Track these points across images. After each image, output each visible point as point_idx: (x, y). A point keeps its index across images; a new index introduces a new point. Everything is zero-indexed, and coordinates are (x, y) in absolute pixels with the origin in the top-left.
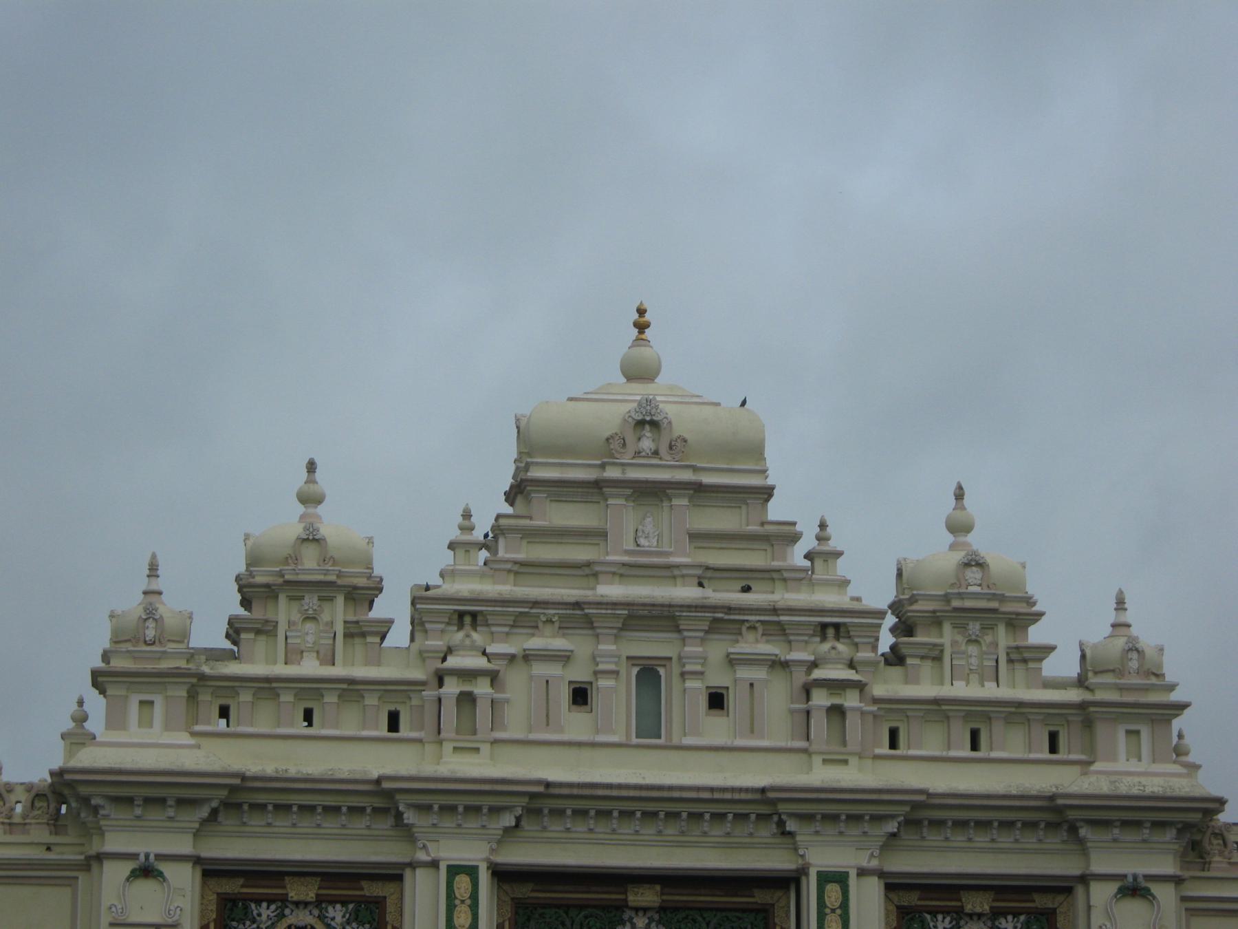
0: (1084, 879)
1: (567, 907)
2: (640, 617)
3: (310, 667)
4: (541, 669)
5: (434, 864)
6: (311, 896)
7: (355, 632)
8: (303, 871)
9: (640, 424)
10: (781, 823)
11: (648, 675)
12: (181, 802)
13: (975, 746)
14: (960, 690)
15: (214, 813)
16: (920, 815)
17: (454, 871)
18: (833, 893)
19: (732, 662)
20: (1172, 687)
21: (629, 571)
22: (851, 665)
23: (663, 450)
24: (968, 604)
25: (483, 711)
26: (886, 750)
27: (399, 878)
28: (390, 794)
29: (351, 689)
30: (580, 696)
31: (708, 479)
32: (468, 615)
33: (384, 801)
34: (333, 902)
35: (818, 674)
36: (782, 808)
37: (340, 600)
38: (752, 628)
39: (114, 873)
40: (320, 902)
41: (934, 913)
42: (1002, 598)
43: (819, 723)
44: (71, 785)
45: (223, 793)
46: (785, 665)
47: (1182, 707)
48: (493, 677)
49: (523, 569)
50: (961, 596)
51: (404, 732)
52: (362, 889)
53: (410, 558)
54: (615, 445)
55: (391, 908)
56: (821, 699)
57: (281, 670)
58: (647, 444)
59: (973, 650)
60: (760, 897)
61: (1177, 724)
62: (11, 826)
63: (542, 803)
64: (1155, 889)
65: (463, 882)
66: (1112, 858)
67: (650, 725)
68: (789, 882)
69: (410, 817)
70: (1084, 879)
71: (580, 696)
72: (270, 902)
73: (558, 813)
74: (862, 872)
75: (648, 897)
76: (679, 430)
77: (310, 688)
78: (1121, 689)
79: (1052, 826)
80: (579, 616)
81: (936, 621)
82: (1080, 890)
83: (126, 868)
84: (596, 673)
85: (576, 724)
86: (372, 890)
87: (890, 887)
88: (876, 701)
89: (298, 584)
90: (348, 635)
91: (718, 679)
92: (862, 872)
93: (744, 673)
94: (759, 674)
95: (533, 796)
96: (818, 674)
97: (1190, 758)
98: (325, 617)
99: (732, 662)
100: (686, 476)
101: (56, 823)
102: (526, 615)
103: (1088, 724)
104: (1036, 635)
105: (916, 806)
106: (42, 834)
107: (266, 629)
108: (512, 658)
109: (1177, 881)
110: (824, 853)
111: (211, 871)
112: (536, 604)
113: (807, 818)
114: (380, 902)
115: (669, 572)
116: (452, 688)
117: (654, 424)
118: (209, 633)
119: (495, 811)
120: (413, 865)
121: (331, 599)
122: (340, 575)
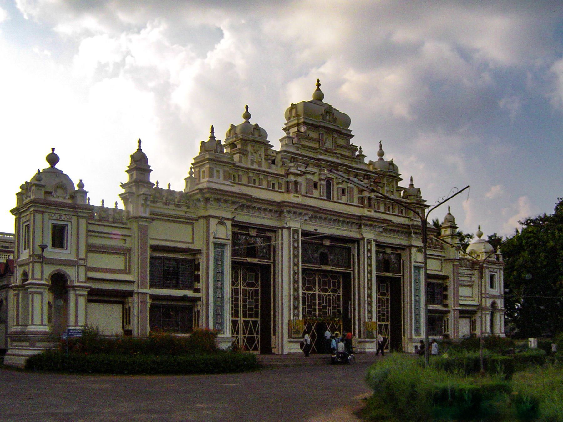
0: (410, 247)
3: (255, 167)
5: (289, 228)
11: (329, 182)
33: (279, 209)
52: (266, 233)
68: (356, 241)
72: (243, 235)
77: (258, 172)
85: (316, 193)
86: (269, 234)
98: (259, 152)
120: (282, 228)
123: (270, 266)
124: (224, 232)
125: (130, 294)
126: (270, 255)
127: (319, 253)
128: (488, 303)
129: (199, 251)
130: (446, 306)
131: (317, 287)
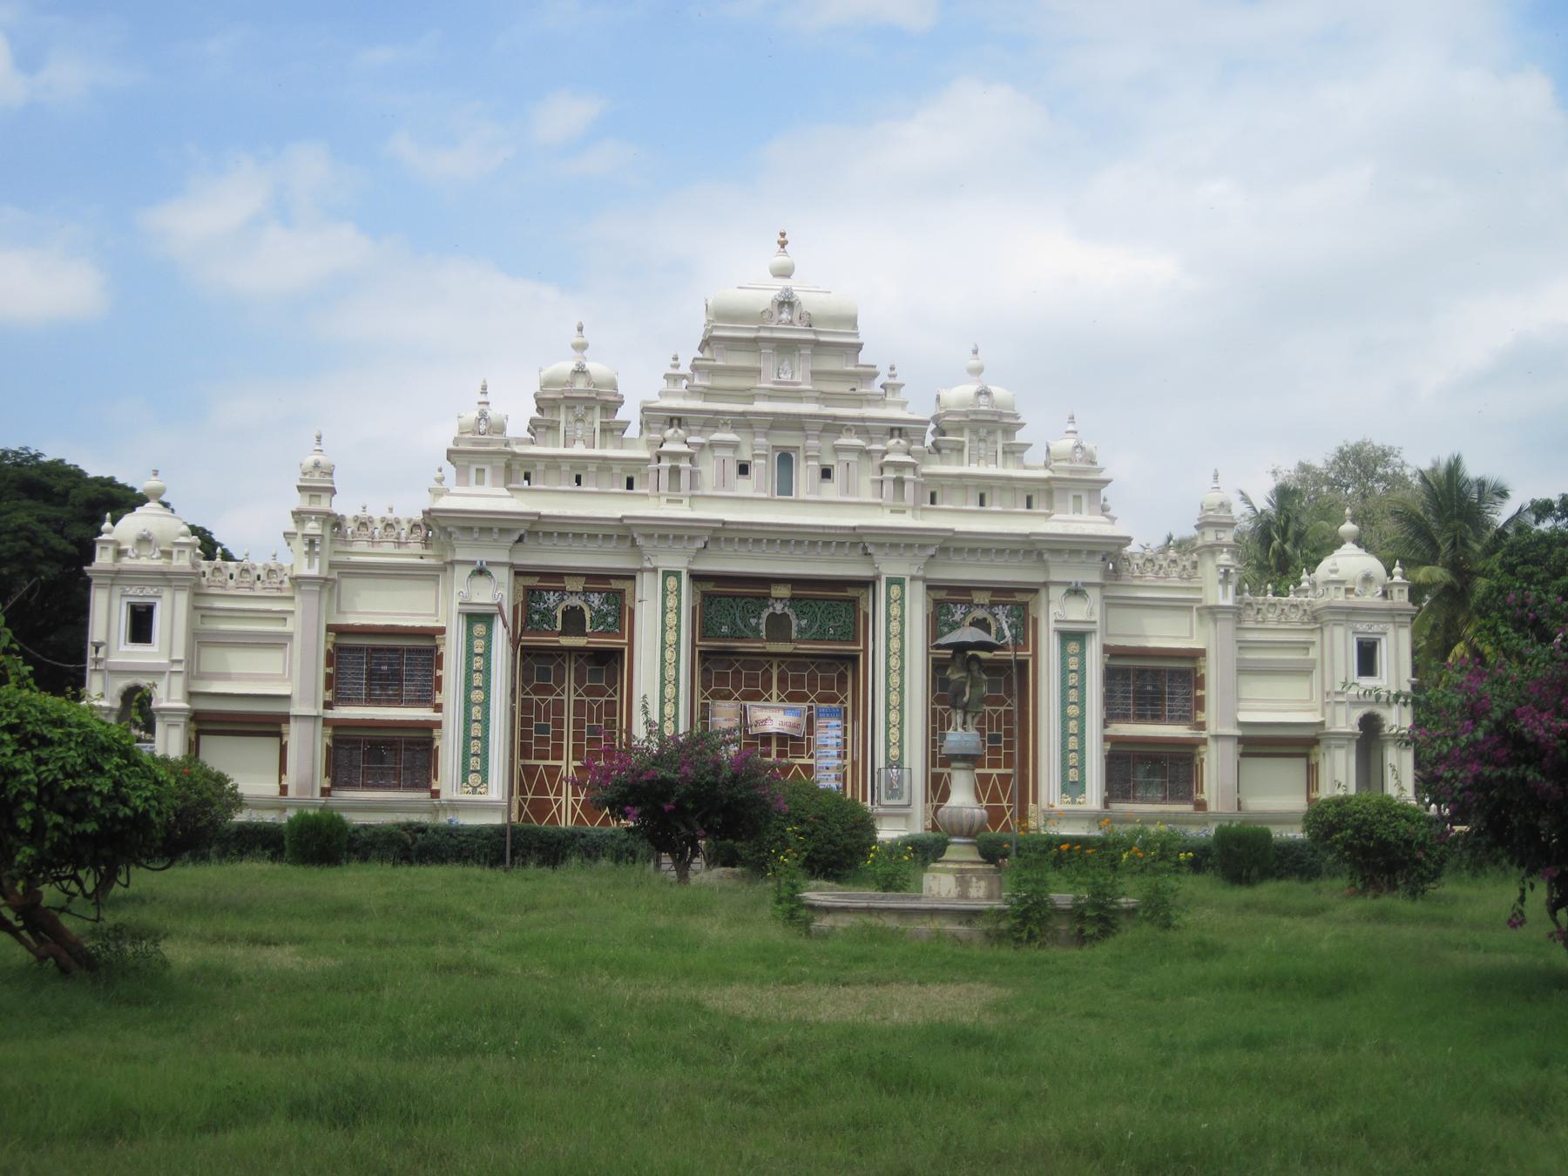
0: (1046, 584)
1: (734, 597)
2: (779, 423)
3: (579, 450)
4: (720, 453)
5: (655, 570)
6: (580, 588)
7: (607, 430)
8: (575, 574)
9: (782, 304)
10: (865, 548)
11: (785, 460)
12: (501, 530)
13: (982, 504)
14: (974, 469)
15: (520, 540)
16: (949, 545)
17: (667, 574)
18: (895, 590)
19: (837, 450)
20: (1101, 470)
21: (771, 396)
22: (908, 453)
23: (796, 320)
24: (980, 417)
25: (685, 478)
26: (928, 505)
27: (633, 578)
28: (628, 527)
29: (605, 464)
30: (743, 469)
31: (823, 338)
32: (676, 419)
33: (624, 533)
34: (593, 591)
35: (888, 458)
36: (865, 539)
37: (598, 410)
38: (849, 430)
39: (462, 573)
40: (585, 591)
41: (955, 603)
42: (1001, 415)
43: (888, 488)
44: (434, 519)
45: (527, 526)
46: (868, 452)
47: (1107, 482)
48: (691, 458)
49: (708, 393)
50: (975, 412)
51: (636, 490)
53: (642, 385)
54: (766, 316)
55: (628, 596)
56: (890, 474)
57: (561, 451)
58: (785, 316)
59: (982, 445)
60: (851, 593)
61: (1104, 492)
62: (399, 544)
63: (720, 535)
64: (1089, 591)
65: (672, 582)
66: (1061, 572)
67: (785, 486)
68: (868, 584)
69: (640, 541)
70: (1046, 584)
71: (743, 469)
73: (729, 541)
74: (913, 578)
75: (783, 591)
76: (806, 308)
78: (1072, 471)
79: (1027, 553)
80: (743, 422)
81: (959, 429)
82: (1043, 593)
83: (469, 570)
84: (754, 456)
85: (745, 487)
86: (616, 585)
87: (929, 588)
88: (923, 475)
89: (576, 402)
90: (603, 431)
91: (828, 461)
92: (913, 578)
93: (844, 457)
94: (852, 458)
95: (715, 529)
96: (888, 458)
97: (1111, 513)
98: (589, 419)
99: (837, 450)
100: (811, 336)
101: (426, 542)
102: (712, 420)
103: (1049, 493)
104: (1020, 437)
105: (946, 539)
106: (417, 548)
107: (552, 427)
108: (702, 446)
109: (1102, 586)
110: (890, 567)
111: (519, 573)
112: (717, 413)
113: (880, 545)
114: (621, 592)
115: (798, 396)
116: (666, 464)
117: (791, 305)
118: (517, 428)
119: (691, 538)
120: (641, 570)
121: (592, 408)
122: (598, 394)
123: (622, 651)
124: (497, 592)
125: (286, 718)
126: (622, 629)
127: (765, 615)
128: (1346, 721)
129: (442, 631)
130: (1201, 726)
131: (775, 690)
